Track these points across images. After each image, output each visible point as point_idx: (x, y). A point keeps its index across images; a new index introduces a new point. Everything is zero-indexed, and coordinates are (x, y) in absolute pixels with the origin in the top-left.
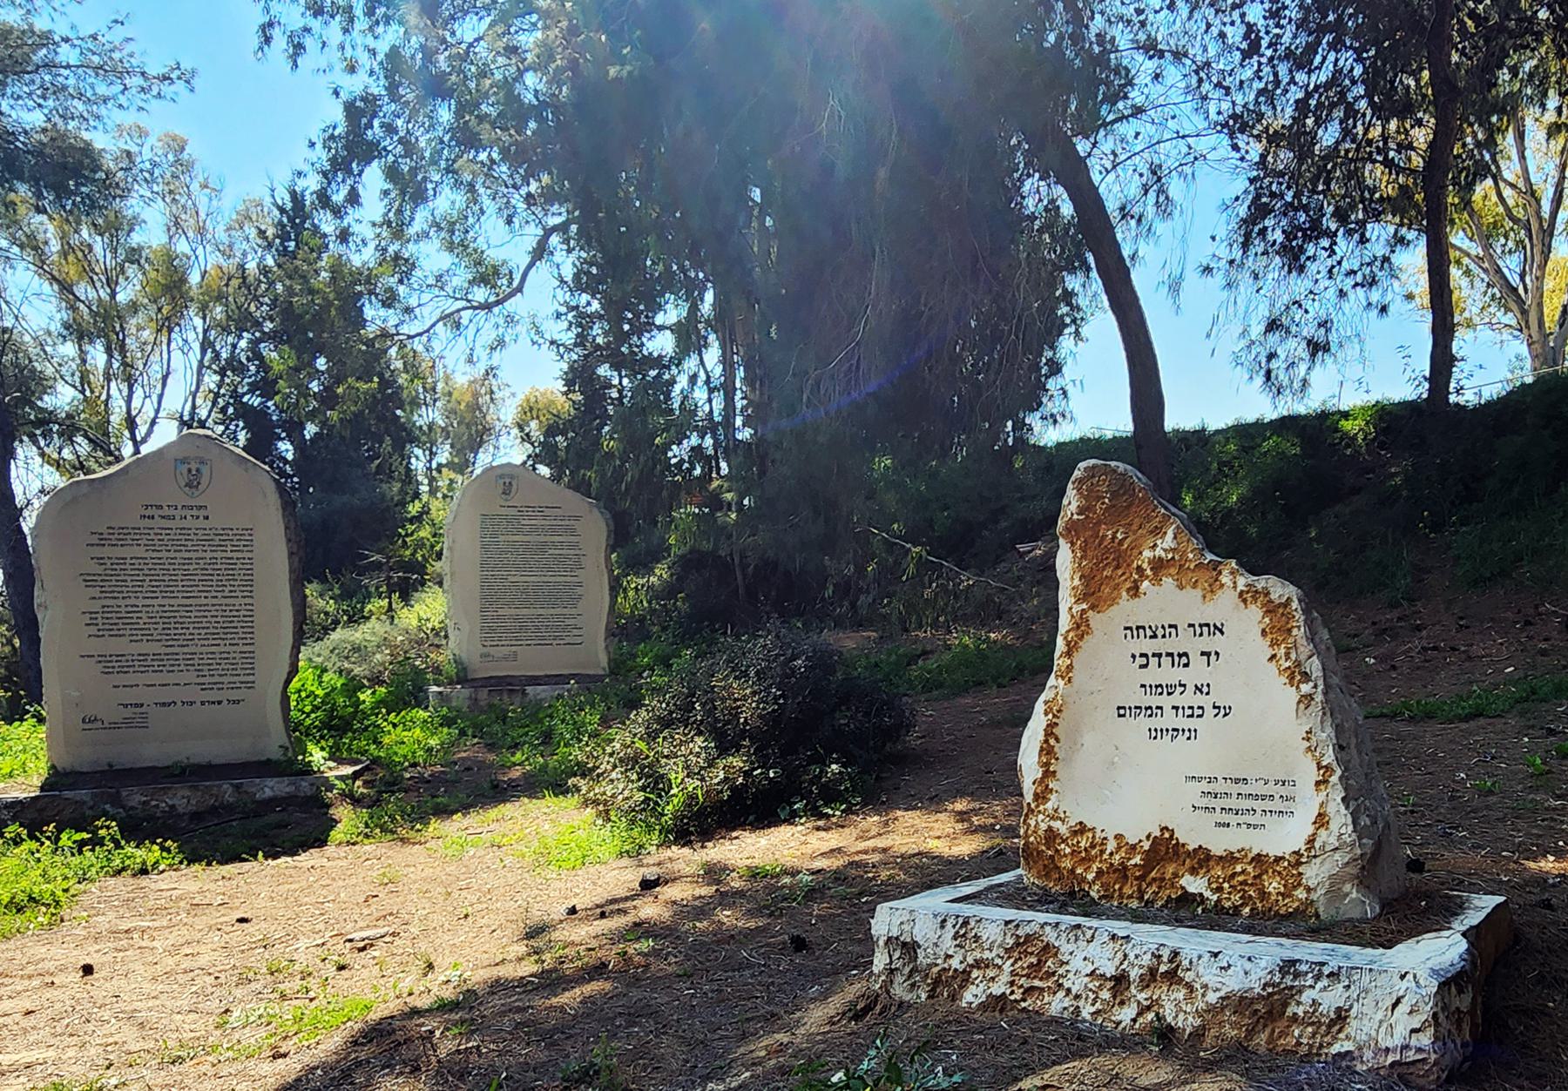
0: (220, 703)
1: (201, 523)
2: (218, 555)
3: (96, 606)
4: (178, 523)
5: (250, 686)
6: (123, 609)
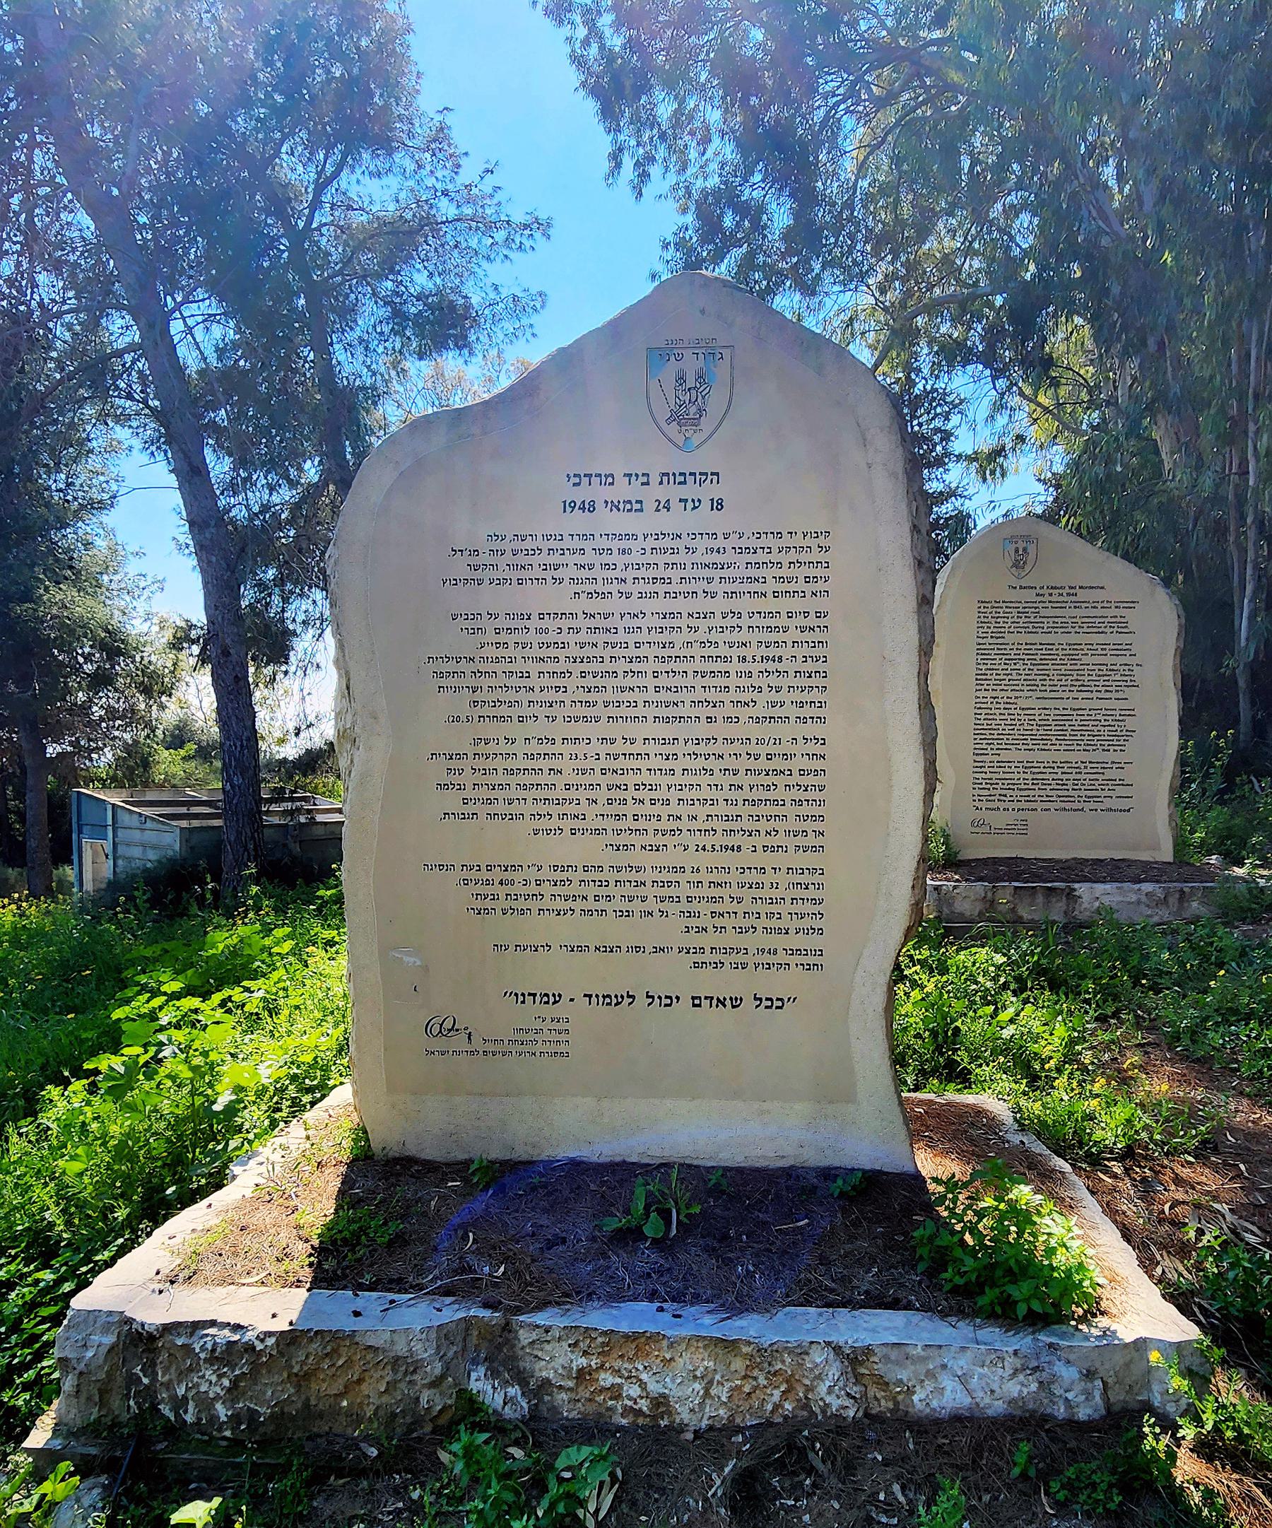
0: (736, 1003)
1: (705, 519)
2: (744, 604)
6: (520, 748)
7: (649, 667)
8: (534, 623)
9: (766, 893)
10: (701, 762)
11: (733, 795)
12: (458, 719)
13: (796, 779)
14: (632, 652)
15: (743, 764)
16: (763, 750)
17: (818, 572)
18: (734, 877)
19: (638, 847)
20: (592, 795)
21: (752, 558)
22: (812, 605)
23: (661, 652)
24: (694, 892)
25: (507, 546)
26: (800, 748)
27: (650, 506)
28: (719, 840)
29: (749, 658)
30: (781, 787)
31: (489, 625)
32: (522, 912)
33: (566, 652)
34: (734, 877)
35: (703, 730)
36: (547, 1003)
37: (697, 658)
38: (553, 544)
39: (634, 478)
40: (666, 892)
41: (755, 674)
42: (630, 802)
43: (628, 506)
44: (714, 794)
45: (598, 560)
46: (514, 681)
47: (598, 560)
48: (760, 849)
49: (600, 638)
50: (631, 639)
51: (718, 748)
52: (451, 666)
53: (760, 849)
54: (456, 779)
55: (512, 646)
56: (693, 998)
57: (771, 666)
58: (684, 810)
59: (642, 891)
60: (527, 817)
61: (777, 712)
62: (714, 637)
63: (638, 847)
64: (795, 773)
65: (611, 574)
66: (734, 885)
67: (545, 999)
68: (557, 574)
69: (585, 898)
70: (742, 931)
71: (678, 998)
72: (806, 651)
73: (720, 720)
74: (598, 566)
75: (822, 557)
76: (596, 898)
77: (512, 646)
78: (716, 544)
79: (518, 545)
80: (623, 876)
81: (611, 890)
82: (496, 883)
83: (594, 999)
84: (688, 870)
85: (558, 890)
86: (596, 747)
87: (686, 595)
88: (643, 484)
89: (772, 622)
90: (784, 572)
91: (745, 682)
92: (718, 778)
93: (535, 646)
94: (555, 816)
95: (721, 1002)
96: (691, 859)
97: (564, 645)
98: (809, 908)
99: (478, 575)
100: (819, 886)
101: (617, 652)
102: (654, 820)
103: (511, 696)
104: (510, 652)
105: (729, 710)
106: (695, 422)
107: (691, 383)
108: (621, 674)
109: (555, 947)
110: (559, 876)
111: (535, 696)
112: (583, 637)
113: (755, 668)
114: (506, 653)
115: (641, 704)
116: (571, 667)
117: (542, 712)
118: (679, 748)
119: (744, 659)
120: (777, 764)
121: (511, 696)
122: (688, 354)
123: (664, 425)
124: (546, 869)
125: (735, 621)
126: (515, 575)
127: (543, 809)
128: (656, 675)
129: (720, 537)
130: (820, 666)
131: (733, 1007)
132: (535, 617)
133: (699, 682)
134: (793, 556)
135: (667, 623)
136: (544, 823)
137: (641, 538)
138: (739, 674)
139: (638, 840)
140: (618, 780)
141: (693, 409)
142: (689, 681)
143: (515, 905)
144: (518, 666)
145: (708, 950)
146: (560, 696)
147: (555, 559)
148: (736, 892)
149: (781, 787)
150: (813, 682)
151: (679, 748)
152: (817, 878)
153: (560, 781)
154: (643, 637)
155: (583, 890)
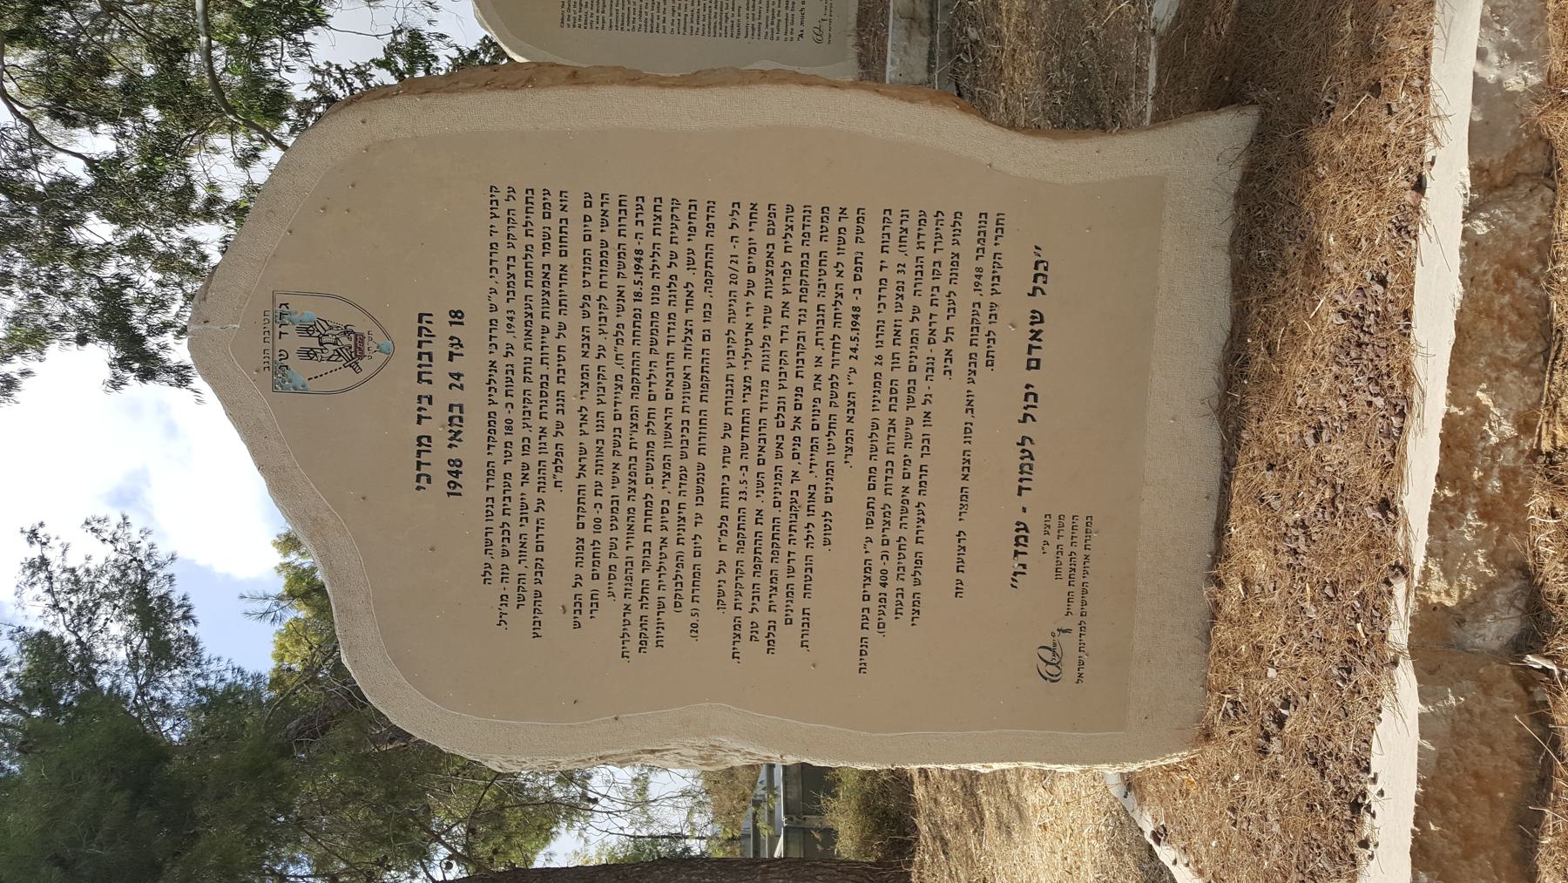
0: (1037, 317)
1: (473, 332)
2: (574, 291)
3: (717, 625)
4: (474, 398)
5: (993, 226)
6: (730, 557)
7: (643, 404)
8: (588, 534)
9: (909, 278)
10: (756, 351)
11: (793, 313)
12: (694, 626)
13: (777, 240)
14: (625, 424)
15: (758, 300)
16: (743, 277)
17: (538, 199)
18: (889, 315)
19: (850, 426)
20: (787, 476)
21: (520, 279)
22: (576, 211)
23: (627, 390)
24: (904, 362)
25: (497, 562)
26: (742, 232)
27: (456, 396)
28: (845, 332)
29: (637, 288)
30: (787, 257)
31: (588, 585)
32: (919, 562)
33: (623, 499)
34: (889, 315)
35: (717, 346)
36: (1026, 539)
37: (635, 348)
38: (498, 509)
39: (423, 413)
40: (902, 395)
41: (656, 282)
42: (797, 433)
43: (456, 421)
44: (792, 335)
45: (518, 458)
46: (654, 560)
47: (518, 458)
48: (857, 285)
49: (608, 460)
50: (610, 424)
51: (739, 328)
52: (634, 630)
53: (857, 285)
54: (763, 631)
55: (613, 561)
56: (1029, 368)
57: (647, 263)
58: (809, 370)
59: (900, 425)
60: (809, 551)
61: (700, 259)
62: (611, 328)
63: (850, 426)
64: (771, 240)
65: (535, 445)
66: (898, 316)
67: (1022, 540)
68: (533, 506)
69: (906, 489)
70: (952, 309)
71: (1027, 386)
72: (630, 221)
73: (707, 326)
74: (525, 459)
75: (521, 196)
76: (907, 476)
77: (613, 561)
78: (503, 322)
79: (497, 548)
80: (882, 445)
81: (898, 459)
82: (883, 590)
83: (1025, 484)
84: (878, 369)
85: (895, 519)
86: (733, 470)
87: (561, 359)
88: (430, 402)
89: (596, 259)
90: (537, 242)
91: (664, 294)
92: (774, 331)
93: (614, 534)
94: (810, 519)
95: (1036, 335)
96: (866, 366)
97: (615, 500)
98: (929, 229)
99: (530, 599)
100: (905, 214)
101: (625, 441)
102: (819, 406)
103: (670, 564)
104: (620, 563)
105: (696, 314)
106: (360, 339)
108: (651, 438)
109: (961, 526)
110: (878, 518)
111: (672, 536)
112: (606, 478)
113: (648, 282)
114: (621, 567)
115: (686, 416)
116: (640, 494)
117: (690, 530)
118: (738, 374)
119: (636, 294)
120: (760, 260)
121: (670, 564)
122: (280, 344)
123: (363, 375)
124: (869, 533)
125: (594, 303)
126: (531, 555)
127: (801, 534)
128: (652, 397)
129: (494, 315)
130: (648, 205)
131: (1042, 321)
132: (581, 533)
133: (662, 347)
134: (519, 231)
135: (593, 380)
136: (818, 532)
137: (493, 408)
138: (655, 300)
139: (842, 426)
140: (771, 447)
141: (344, 340)
142: (661, 360)
143: (910, 569)
144: (637, 553)
145: (973, 349)
146: (673, 508)
147: (515, 507)
148: (907, 314)
149: (787, 257)
150: (666, 213)
151: (738, 374)
152: (895, 218)
153: (769, 513)
154: (608, 410)
155: (897, 490)
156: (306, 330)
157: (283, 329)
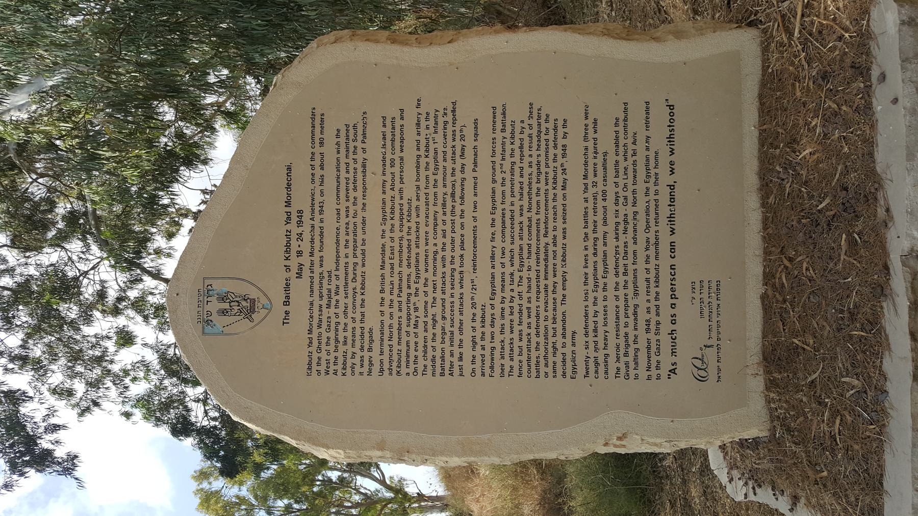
107: (226, 306)
122: (207, 308)
156: (222, 299)
157: (209, 299)
